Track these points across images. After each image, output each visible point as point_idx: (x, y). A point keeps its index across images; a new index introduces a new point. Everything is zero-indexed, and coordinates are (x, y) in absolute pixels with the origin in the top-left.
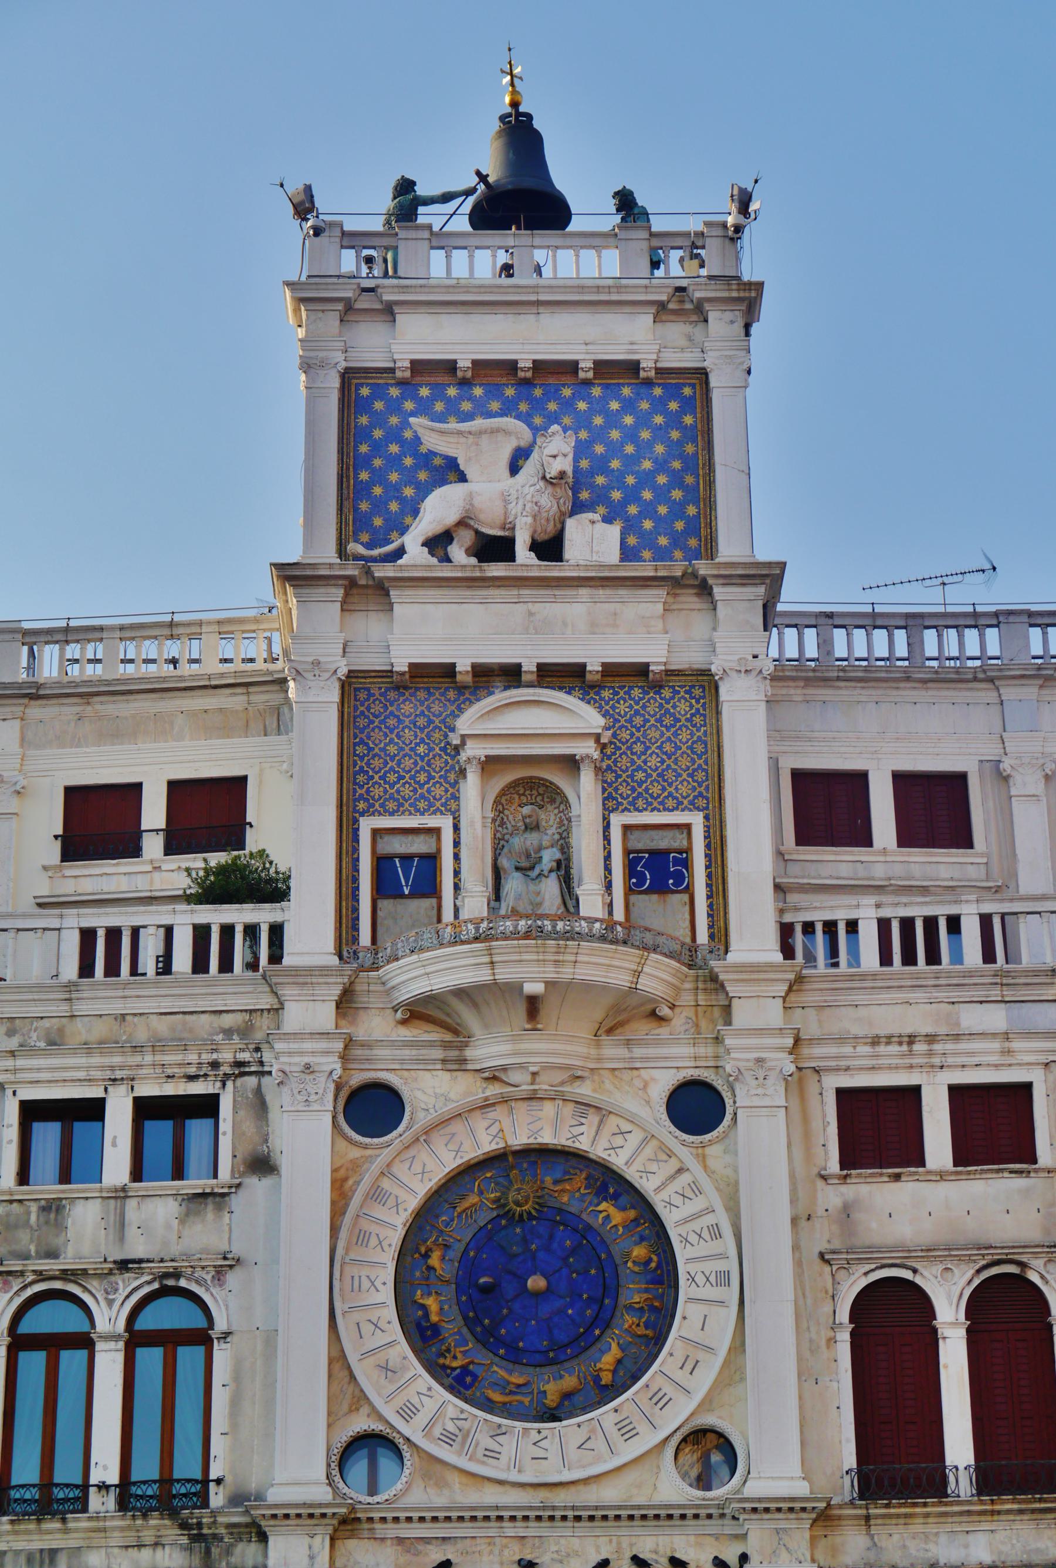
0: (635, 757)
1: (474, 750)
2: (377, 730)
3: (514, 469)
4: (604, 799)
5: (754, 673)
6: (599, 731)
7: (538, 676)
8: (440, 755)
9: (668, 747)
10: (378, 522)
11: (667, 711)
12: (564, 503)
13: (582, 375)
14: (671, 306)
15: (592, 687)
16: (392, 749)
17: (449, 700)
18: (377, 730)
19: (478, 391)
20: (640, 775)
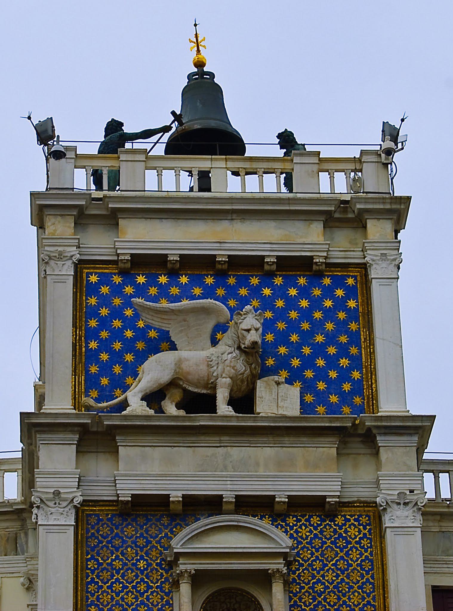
1: (186, 566)
2: (105, 549)
3: (214, 342)
4: (291, 606)
5: (410, 505)
6: (288, 550)
7: (235, 506)
8: (156, 569)
9: (341, 564)
10: (105, 381)
11: (340, 535)
12: (255, 368)
13: (266, 267)
14: (337, 215)
15: (279, 515)
16: (118, 564)
17: (163, 525)
18: (105, 549)
19: (184, 280)
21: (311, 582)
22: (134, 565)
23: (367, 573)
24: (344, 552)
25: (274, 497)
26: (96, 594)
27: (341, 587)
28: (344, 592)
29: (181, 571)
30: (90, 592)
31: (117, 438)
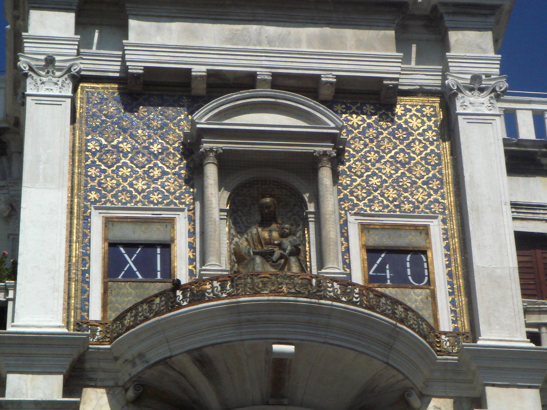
0: (369, 164)
8: (174, 154)
9: (401, 157)
16: (126, 147)
20: (375, 181)
21: (365, 175)
22: (147, 148)
23: (434, 167)
24: (405, 144)
25: (319, 76)
26: (98, 179)
27: (401, 182)
28: (405, 187)
29: (206, 150)
30: (90, 176)
31: (127, 5)
